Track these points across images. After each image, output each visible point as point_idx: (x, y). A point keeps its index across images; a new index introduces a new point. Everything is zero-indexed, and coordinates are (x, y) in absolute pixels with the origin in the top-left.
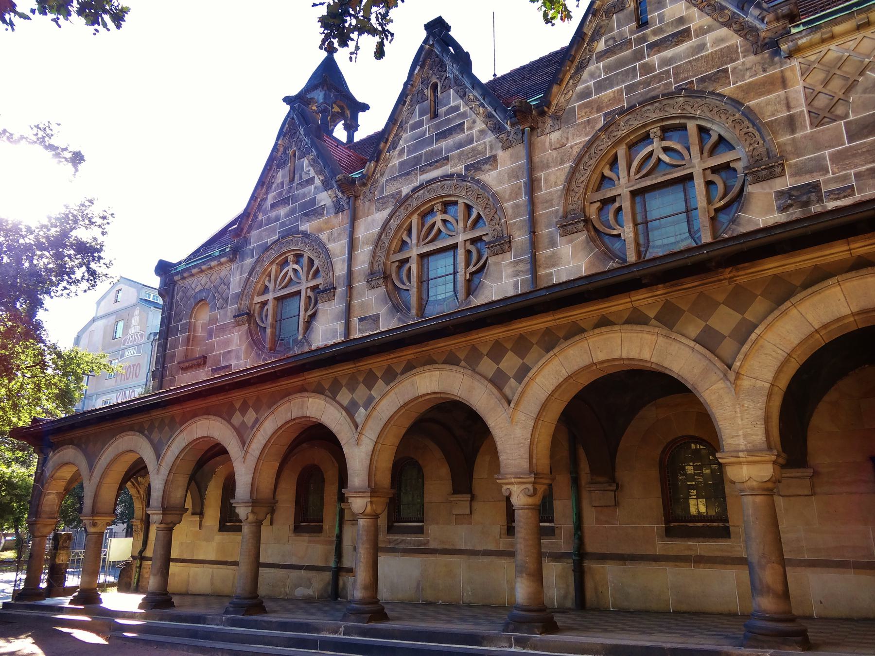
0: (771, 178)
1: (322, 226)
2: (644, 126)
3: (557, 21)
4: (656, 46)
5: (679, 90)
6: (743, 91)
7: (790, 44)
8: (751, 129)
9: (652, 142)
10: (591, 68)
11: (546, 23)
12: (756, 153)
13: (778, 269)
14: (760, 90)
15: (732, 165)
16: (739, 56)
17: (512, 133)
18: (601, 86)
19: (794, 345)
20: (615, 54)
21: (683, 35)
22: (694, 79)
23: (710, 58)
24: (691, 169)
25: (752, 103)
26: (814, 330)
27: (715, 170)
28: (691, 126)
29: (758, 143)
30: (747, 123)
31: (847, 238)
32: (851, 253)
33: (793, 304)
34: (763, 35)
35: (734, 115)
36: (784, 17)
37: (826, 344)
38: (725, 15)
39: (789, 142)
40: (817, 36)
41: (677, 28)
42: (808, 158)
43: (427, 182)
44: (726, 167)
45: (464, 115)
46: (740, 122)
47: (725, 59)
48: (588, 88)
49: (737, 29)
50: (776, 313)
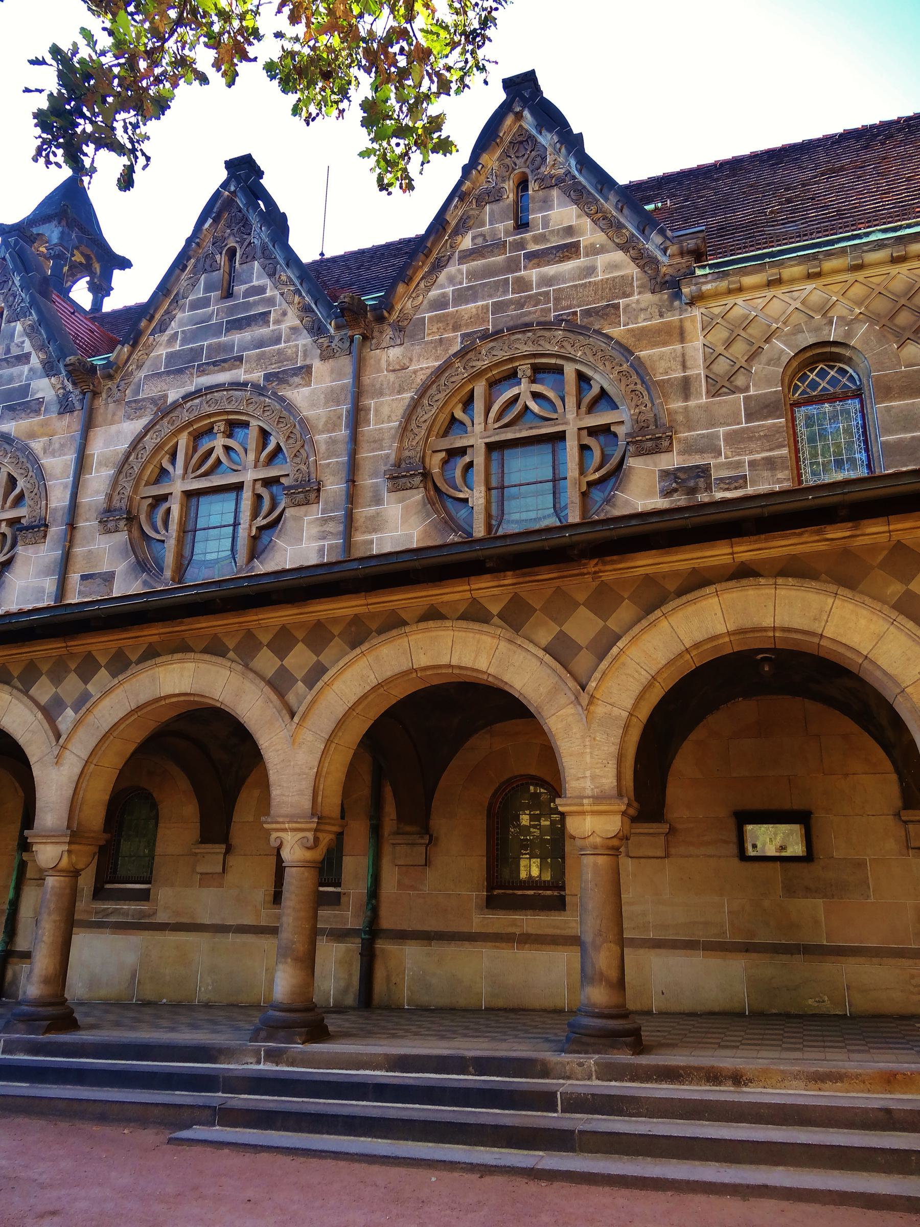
0: (657, 452)
1: (35, 429)
2: (511, 360)
3: (396, 189)
4: (537, 258)
5: (559, 320)
6: (634, 336)
7: (693, 288)
8: (639, 387)
9: (519, 383)
10: (451, 269)
11: (381, 190)
13: (649, 567)
15: (613, 428)
17: (337, 339)
18: (462, 297)
19: (660, 666)
20: (484, 257)
21: (570, 250)
22: (578, 310)
25: (642, 354)
26: (683, 648)
27: (593, 431)
28: (569, 369)
29: (646, 406)
30: (635, 377)
31: (731, 538)
32: (733, 558)
33: (664, 614)
35: (621, 365)
36: (690, 252)
37: (697, 668)
39: (681, 410)
40: (723, 285)
42: (700, 434)
43: (207, 388)
44: (604, 431)
45: (271, 301)
46: (627, 375)
47: (617, 291)
48: (444, 295)
50: (644, 623)
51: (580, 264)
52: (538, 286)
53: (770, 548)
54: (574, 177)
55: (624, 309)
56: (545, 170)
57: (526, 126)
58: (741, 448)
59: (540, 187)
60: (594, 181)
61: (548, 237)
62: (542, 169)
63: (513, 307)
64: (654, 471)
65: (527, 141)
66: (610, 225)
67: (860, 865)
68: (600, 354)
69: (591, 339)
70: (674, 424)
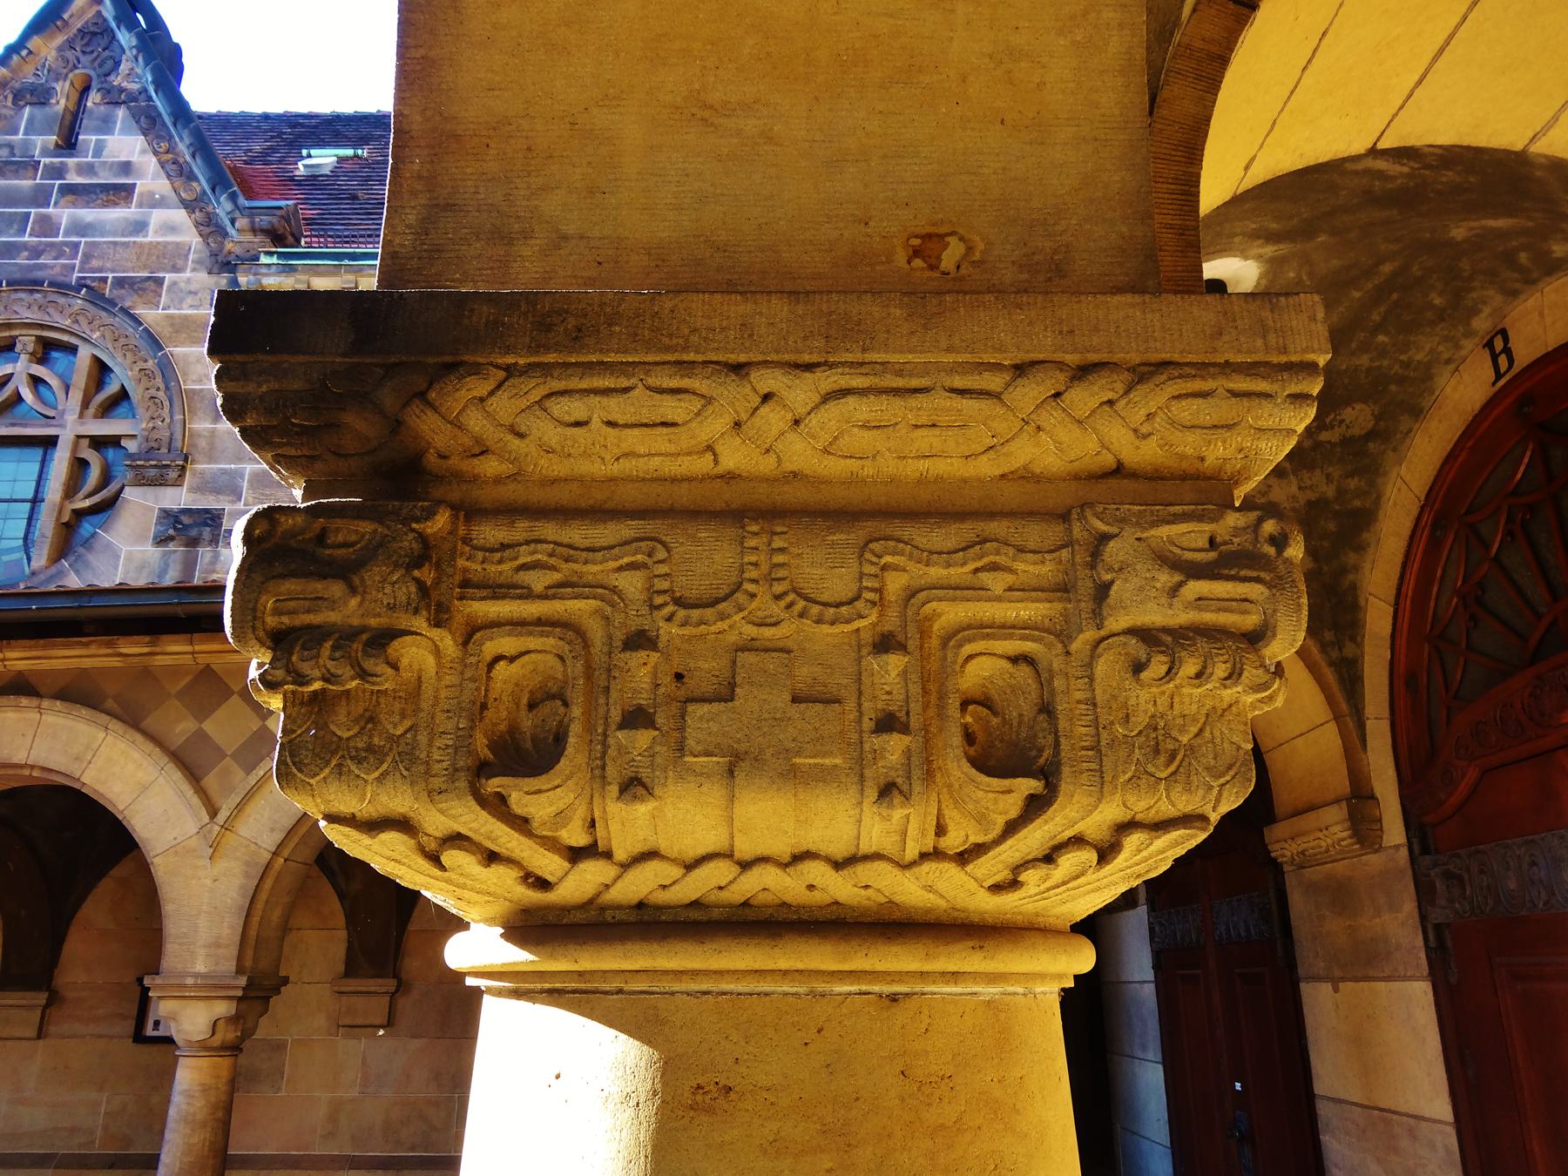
0: (161, 485)
4: (73, 192)
5: (81, 284)
6: (172, 325)
7: (251, 277)
8: (161, 394)
9: (16, 360)
12: (155, 435)
14: (196, 334)
15: (123, 443)
16: (187, 265)
21: (120, 193)
22: (111, 275)
23: (146, 251)
24: (58, 429)
25: (178, 350)
27: (99, 443)
28: (85, 353)
29: (163, 421)
30: (159, 381)
34: (229, 246)
35: (146, 361)
36: (264, 232)
38: (191, 190)
39: (206, 434)
41: (116, 176)
42: (221, 469)
44: (114, 441)
46: (150, 376)
47: (166, 261)
49: (199, 220)
51: (128, 216)
52: (67, 234)
53: (50, 658)
54: (150, 99)
55: (169, 288)
56: (117, 80)
57: (106, 14)
58: (267, 495)
59: (103, 99)
60: (169, 111)
61: (96, 170)
62: (112, 77)
63: (26, 254)
64: (152, 509)
65: (101, 34)
66: (179, 172)
67: (280, 1047)
68: (123, 341)
69: (117, 319)
70: (193, 452)
